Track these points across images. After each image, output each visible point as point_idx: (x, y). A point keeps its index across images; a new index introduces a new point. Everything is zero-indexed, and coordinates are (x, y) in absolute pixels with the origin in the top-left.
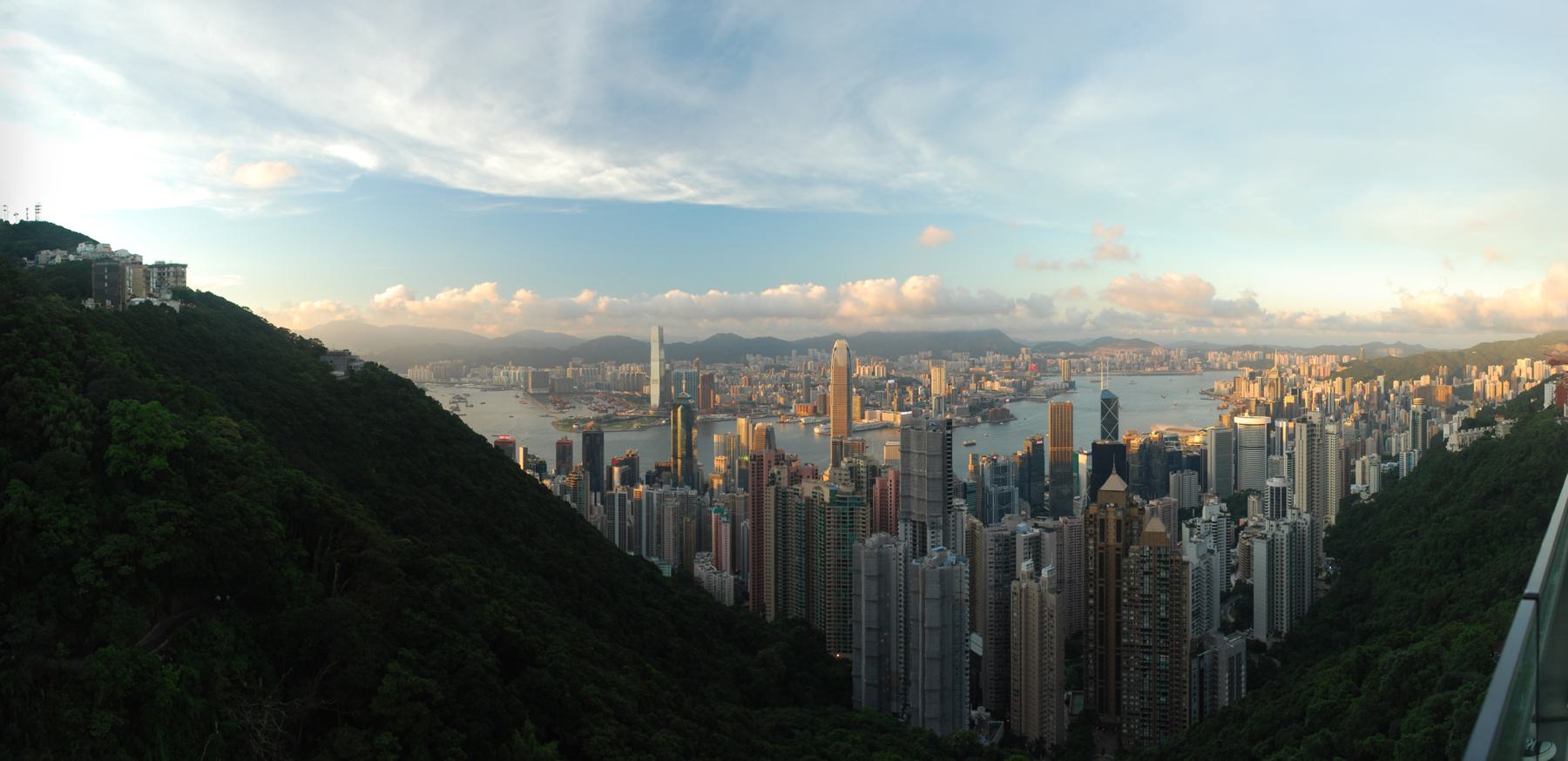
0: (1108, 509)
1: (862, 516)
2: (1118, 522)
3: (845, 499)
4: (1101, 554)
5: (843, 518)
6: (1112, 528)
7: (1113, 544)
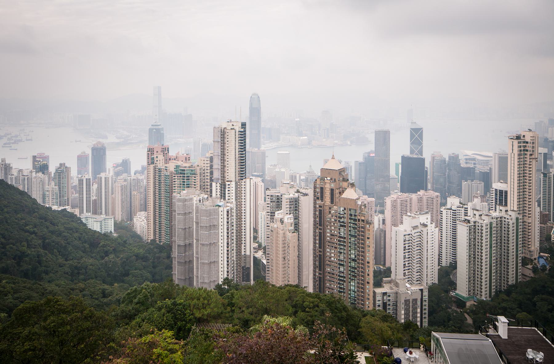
0: (326, 181)
1: (193, 181)
2: (332, 190)
3: (184, 170)
4: (320, 211)
5: (183, 182)
6: (329, 194)
7: (328, 205)
